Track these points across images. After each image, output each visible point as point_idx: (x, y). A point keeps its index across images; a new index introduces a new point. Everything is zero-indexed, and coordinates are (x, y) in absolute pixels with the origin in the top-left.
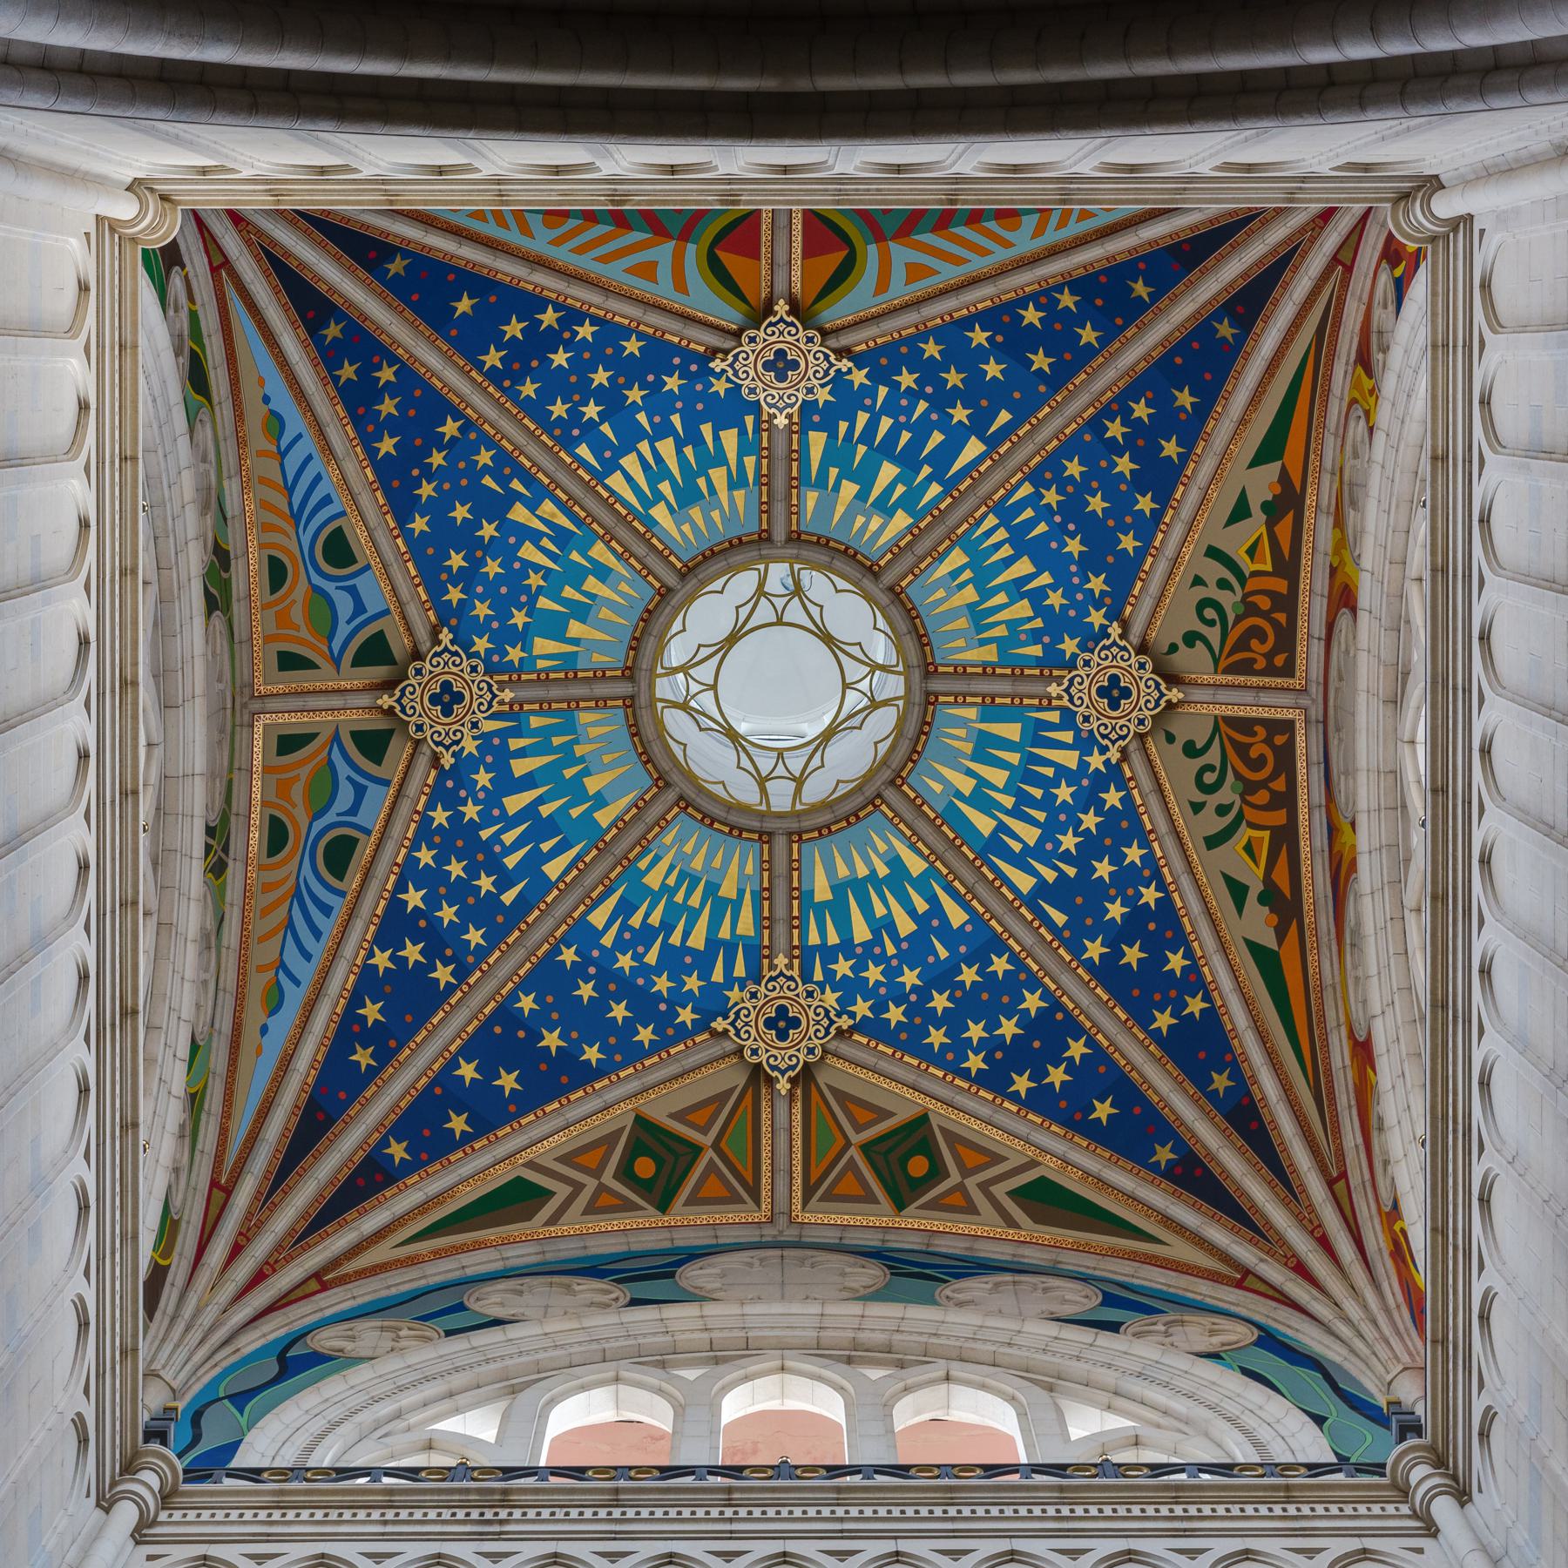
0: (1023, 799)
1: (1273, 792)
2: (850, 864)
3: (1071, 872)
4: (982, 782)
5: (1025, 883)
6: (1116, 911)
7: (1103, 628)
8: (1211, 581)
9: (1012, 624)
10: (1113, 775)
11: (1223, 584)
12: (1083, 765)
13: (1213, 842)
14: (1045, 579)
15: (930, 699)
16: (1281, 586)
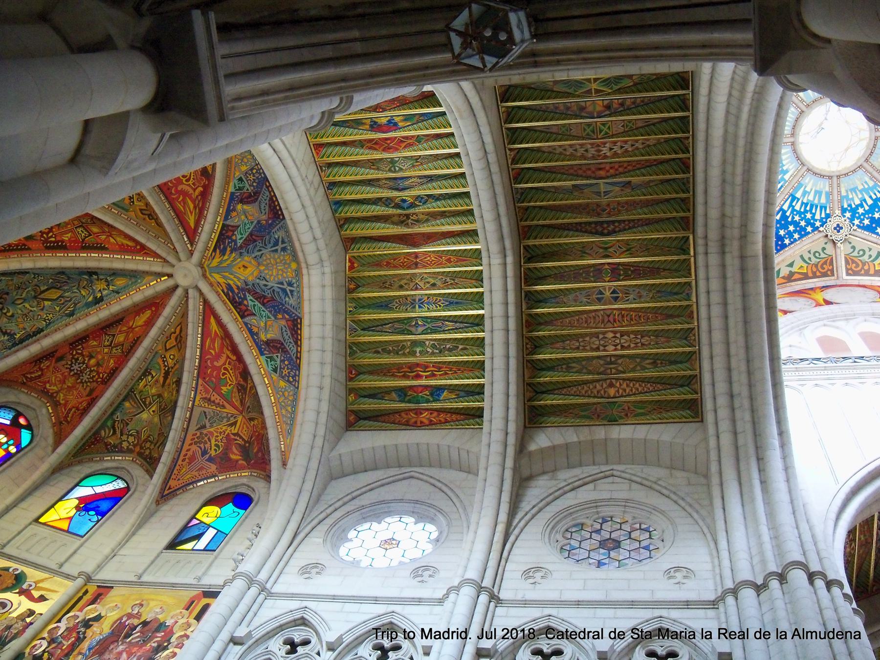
0: (806, 205)
1: (815, 272)
2: (786, 159)
3: (790, 220)
4: (809, 193)
5: (785, 207)
6: (782, 233)
7: (853, 224)
8: (871, 253)
9: (853, 199)
10: (816, 229)
11: (870, 256)
12: (816, 220)
13: (802, 257)
14: (867, 208)
15: (830, 177)
16: (872, 272)
